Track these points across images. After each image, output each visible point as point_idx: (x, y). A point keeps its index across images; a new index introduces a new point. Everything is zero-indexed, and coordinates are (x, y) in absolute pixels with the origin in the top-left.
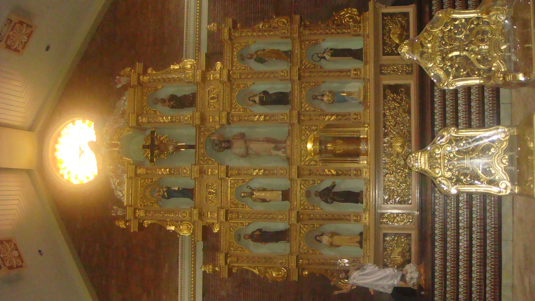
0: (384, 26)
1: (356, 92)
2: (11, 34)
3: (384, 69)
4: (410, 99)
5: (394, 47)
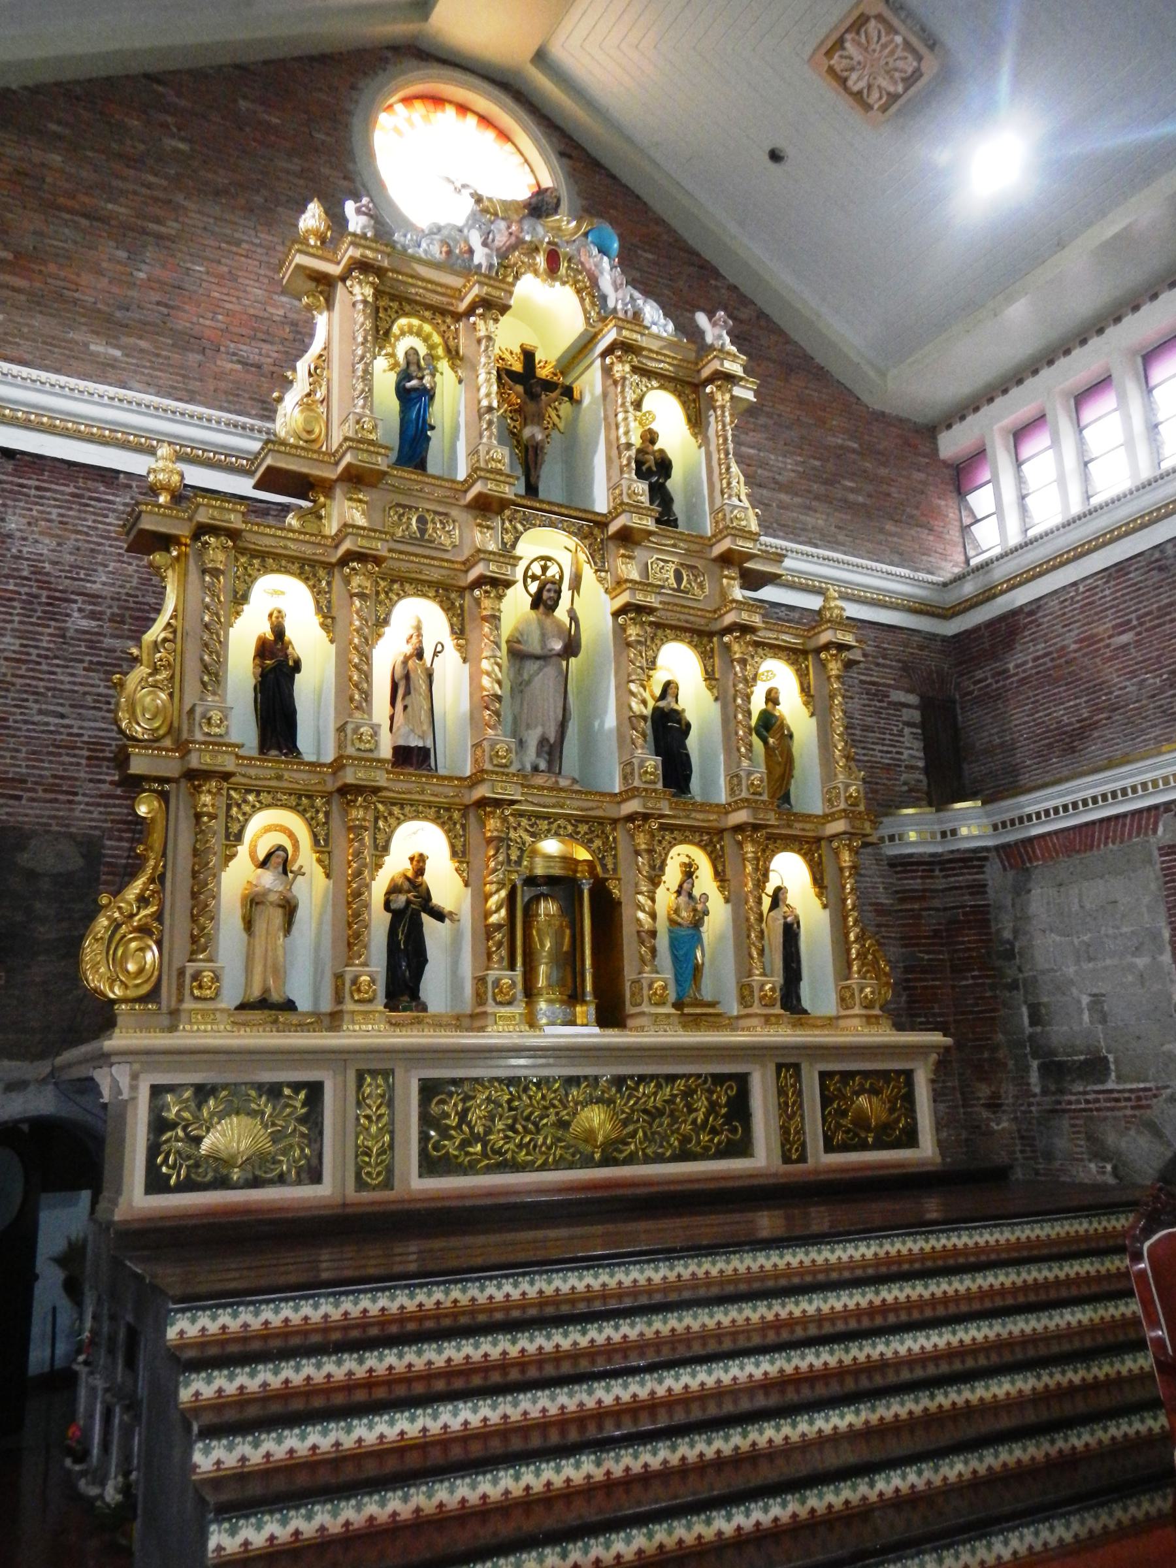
0: (885, 1075)
2: (898, 39)
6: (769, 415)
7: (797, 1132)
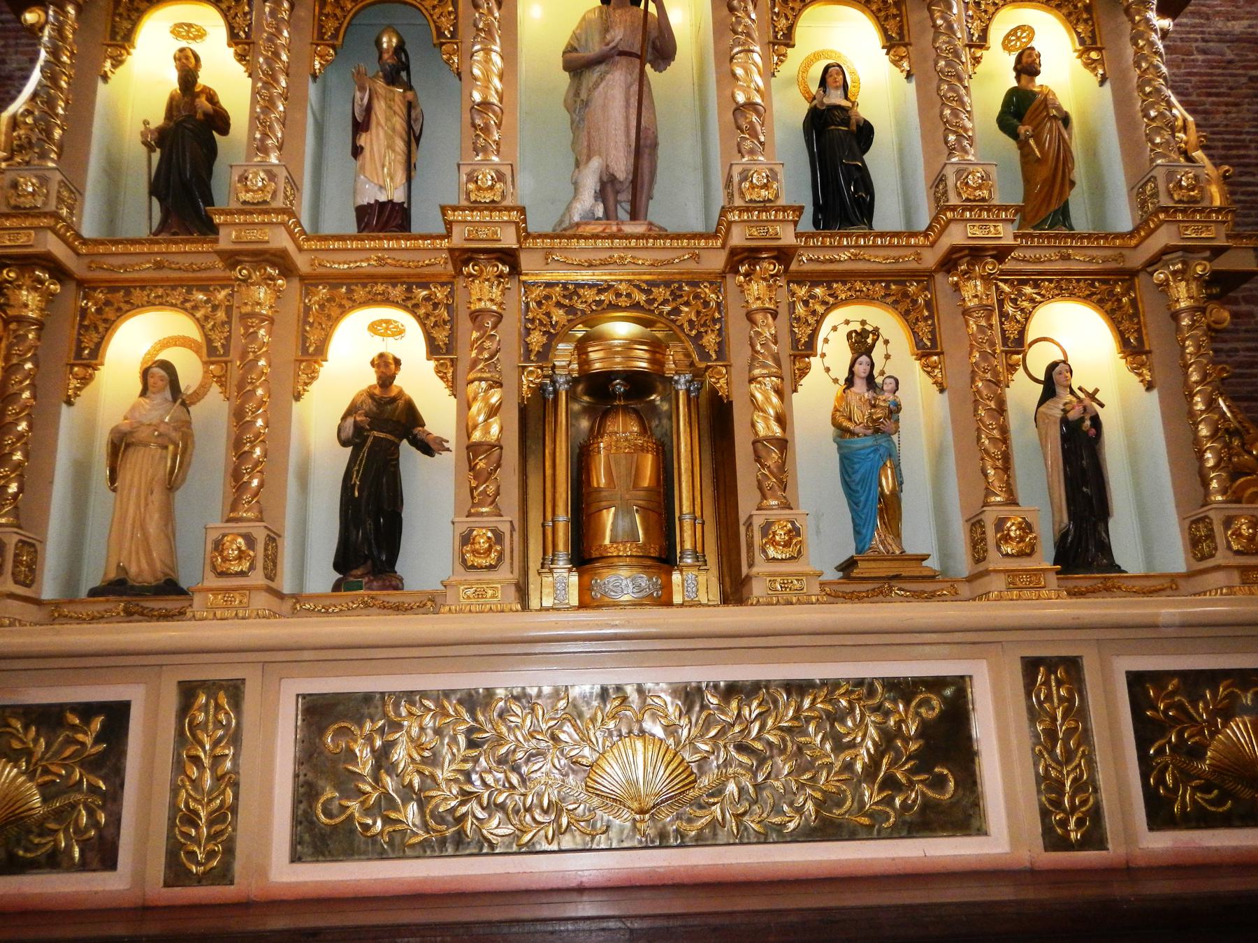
1: (900, 545)
3: (1059, 683)
4: (897, 832)
5: (1180, 735)
7: (1079, 787)
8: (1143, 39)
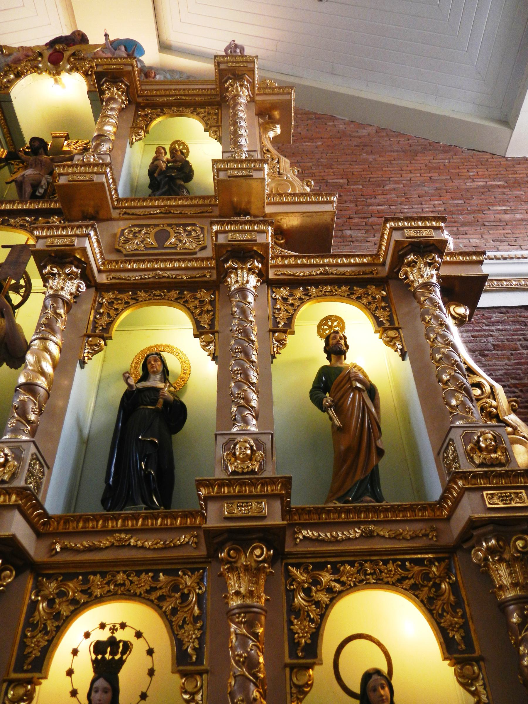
6: (396, 182)
8: (428, 315)
